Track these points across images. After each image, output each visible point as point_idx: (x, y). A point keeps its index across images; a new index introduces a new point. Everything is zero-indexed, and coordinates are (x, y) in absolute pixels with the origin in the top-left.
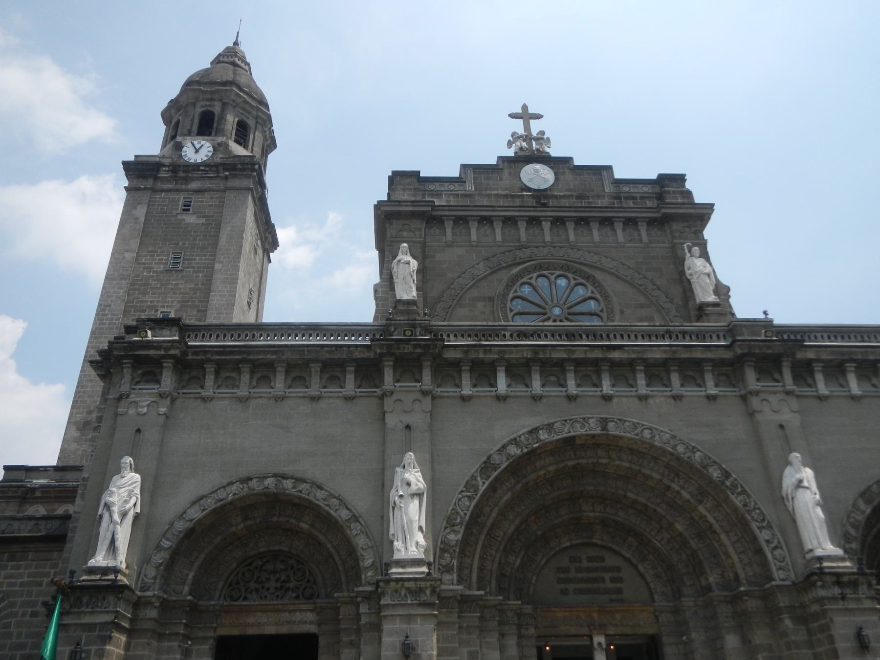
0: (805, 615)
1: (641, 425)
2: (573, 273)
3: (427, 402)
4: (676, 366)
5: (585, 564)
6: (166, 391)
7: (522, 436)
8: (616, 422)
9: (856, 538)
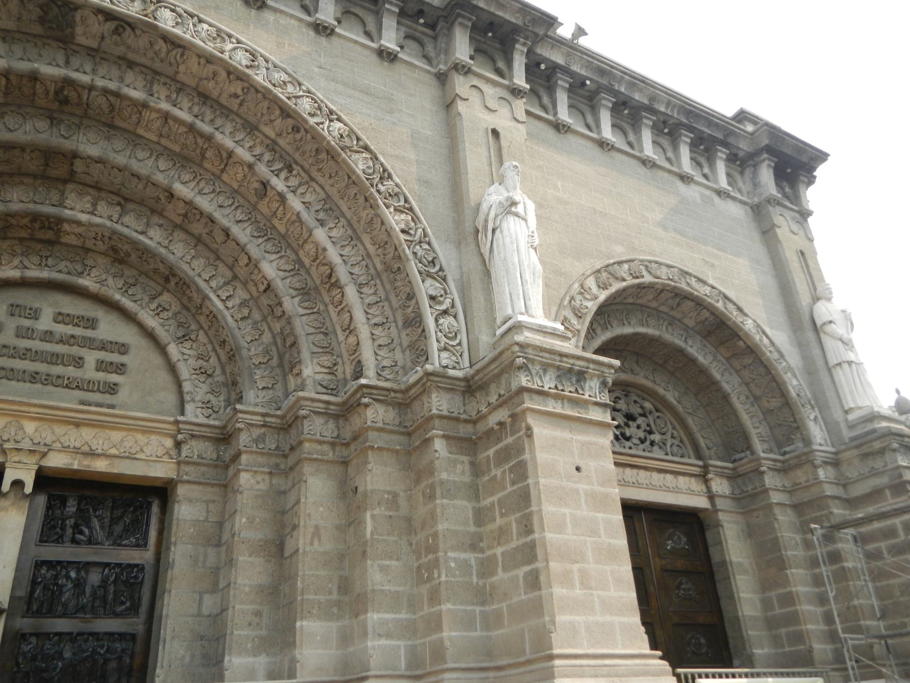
0: (474, 437)
5: (45, 323)
8: (180, 16)
9: (578, 331)
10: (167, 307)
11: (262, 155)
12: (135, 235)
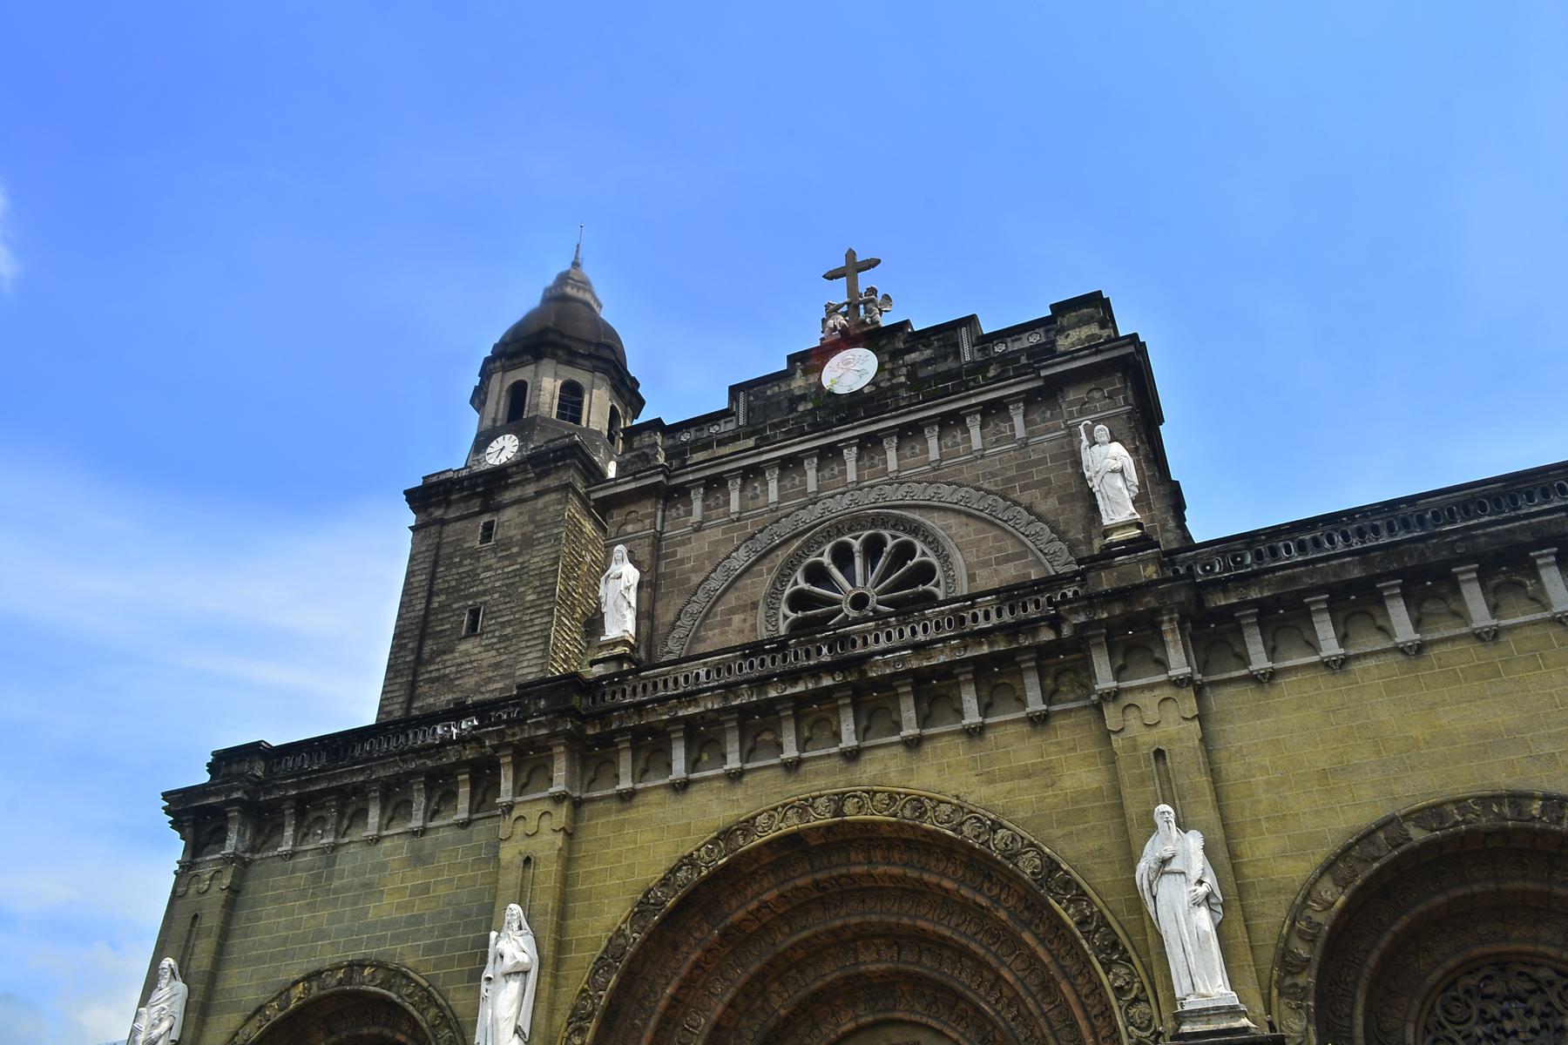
1: (902, 796)
2: (893, 527)
3: (561, 815)
4: (967, 673)
6: (229, 854)
7: (703, 849)
10: (964, 1014)
11: (964, 875)
12: (911, 967)
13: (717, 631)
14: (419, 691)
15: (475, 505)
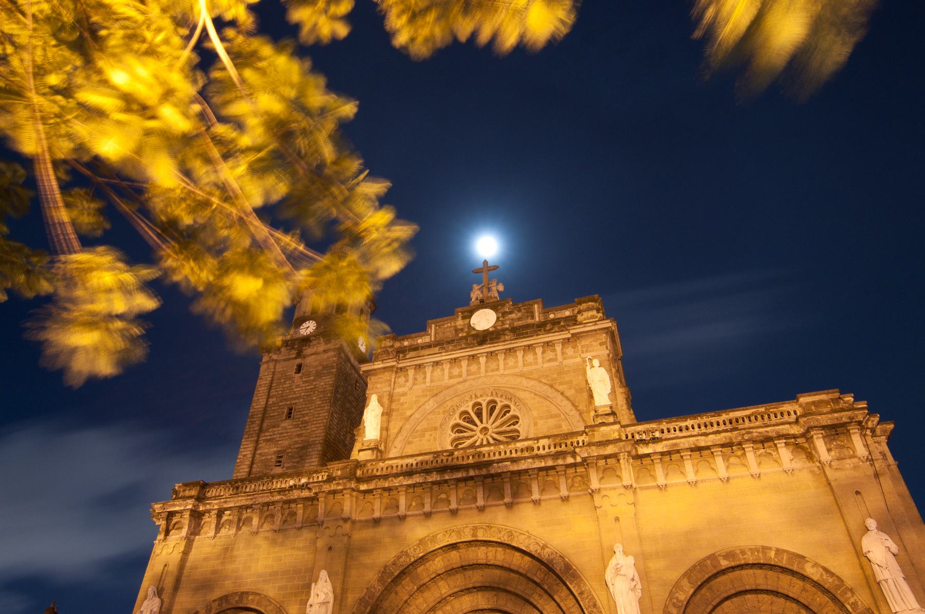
13: (417, 439)
14: (260, 445)
15: (293, 353)
